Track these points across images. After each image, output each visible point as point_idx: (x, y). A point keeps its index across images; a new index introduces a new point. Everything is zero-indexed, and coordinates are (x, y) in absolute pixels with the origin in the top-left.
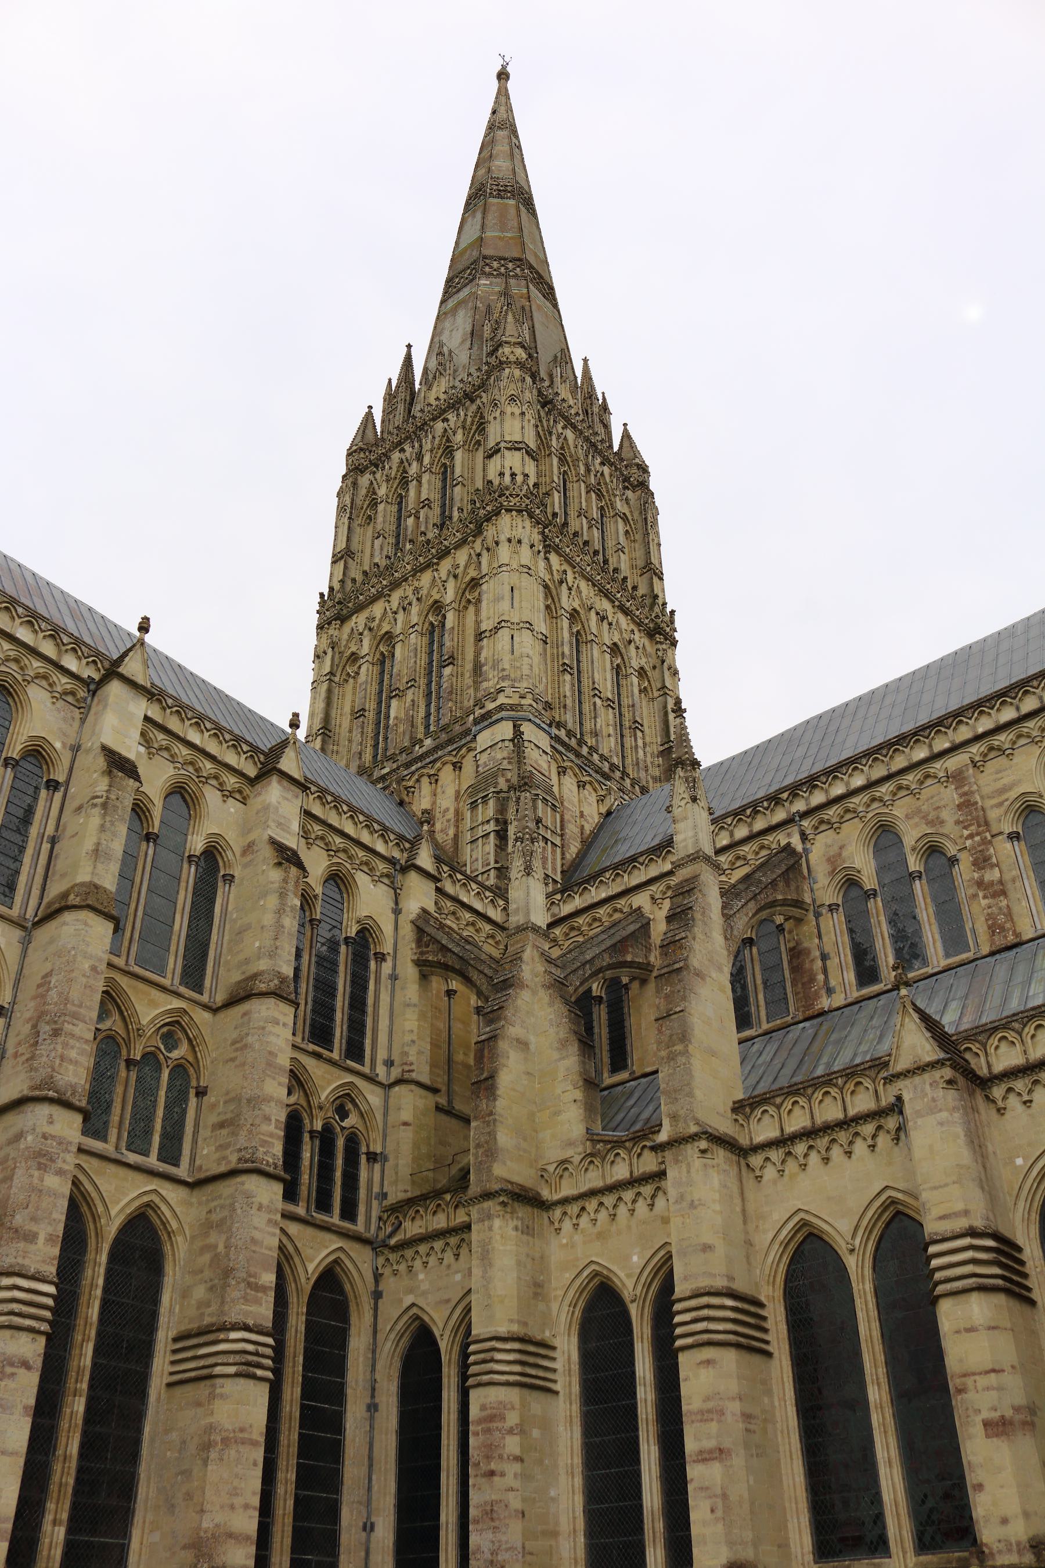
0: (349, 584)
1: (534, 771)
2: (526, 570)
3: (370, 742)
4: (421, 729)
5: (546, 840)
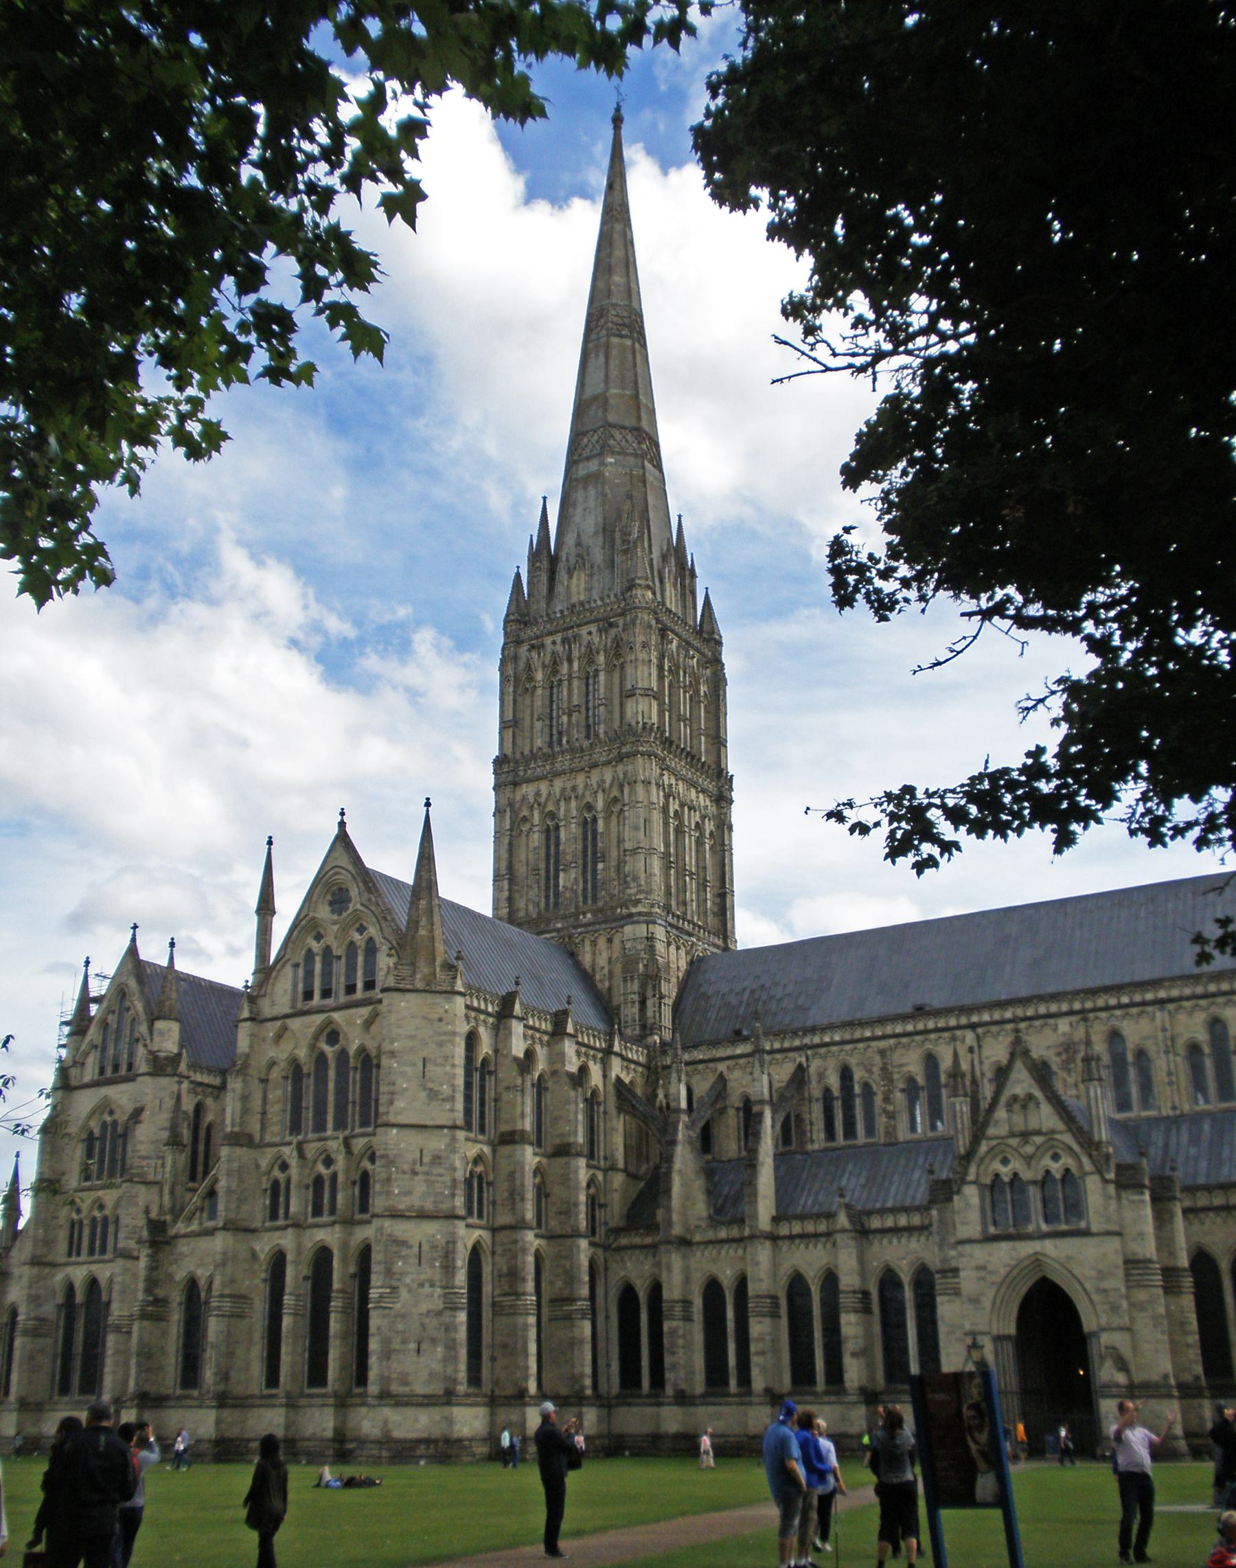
0: (518, 756)
3: (543, 894)
4: (581, 899)
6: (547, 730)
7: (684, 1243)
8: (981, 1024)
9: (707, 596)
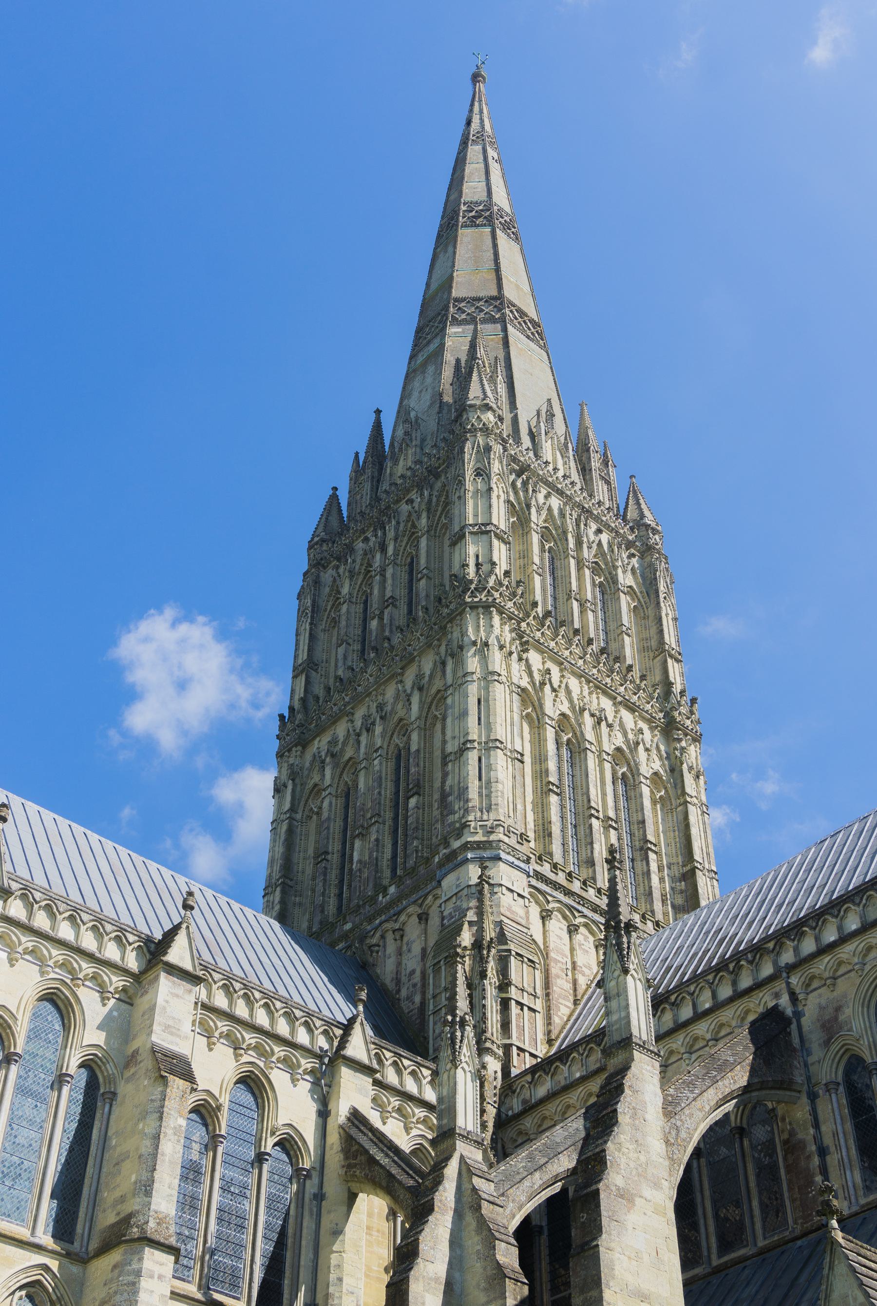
1: (506, 920)
3: (334, 891)
4: (387, 873)
5: (521, 1005)
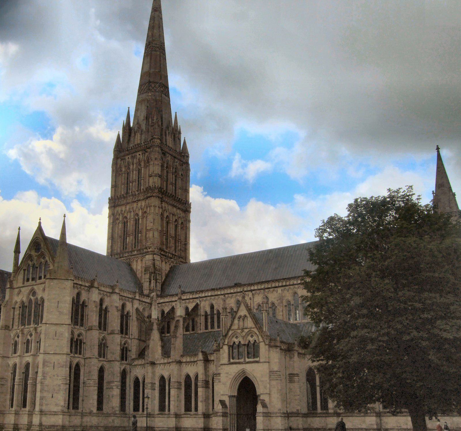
2: (157, 214)
3: (122, 244)
4: (134, 246)
5: (158, 282)
6: (126, 188)
7: (153, 364)
8: (254, 290)
9: (185, 140)
